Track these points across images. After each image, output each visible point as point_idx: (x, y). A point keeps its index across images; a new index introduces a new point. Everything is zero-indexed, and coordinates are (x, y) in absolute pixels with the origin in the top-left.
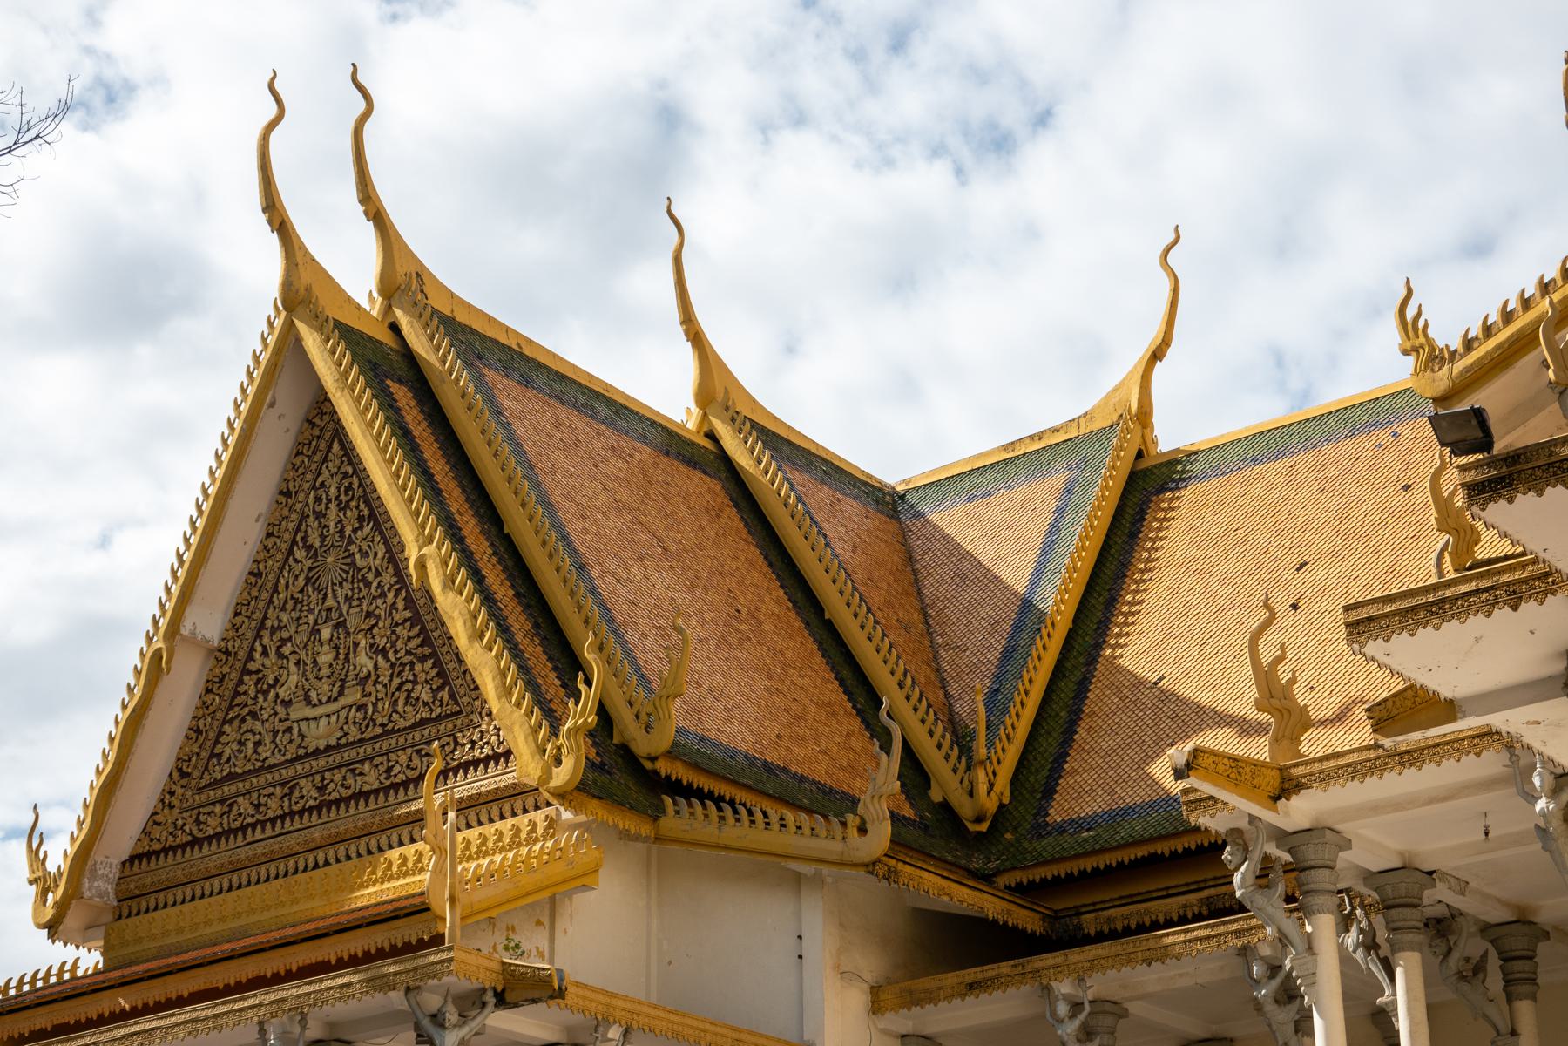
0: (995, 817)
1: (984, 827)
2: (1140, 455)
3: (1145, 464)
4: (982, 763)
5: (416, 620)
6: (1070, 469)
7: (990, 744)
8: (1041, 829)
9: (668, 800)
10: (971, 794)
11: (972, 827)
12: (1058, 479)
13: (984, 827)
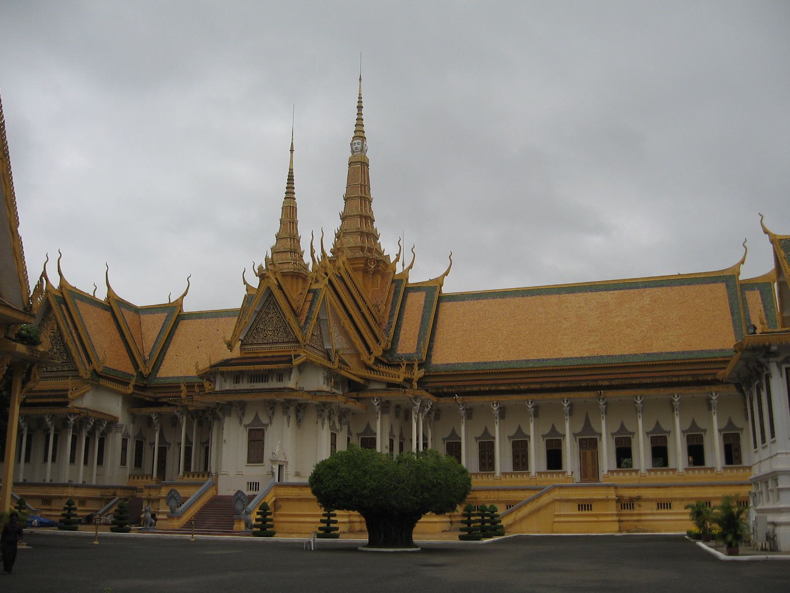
2: (180, 312)
3: (181, 313)
5: (64, 346)
8: (155, 378)
9: (101, 379)
12: (166, 314)
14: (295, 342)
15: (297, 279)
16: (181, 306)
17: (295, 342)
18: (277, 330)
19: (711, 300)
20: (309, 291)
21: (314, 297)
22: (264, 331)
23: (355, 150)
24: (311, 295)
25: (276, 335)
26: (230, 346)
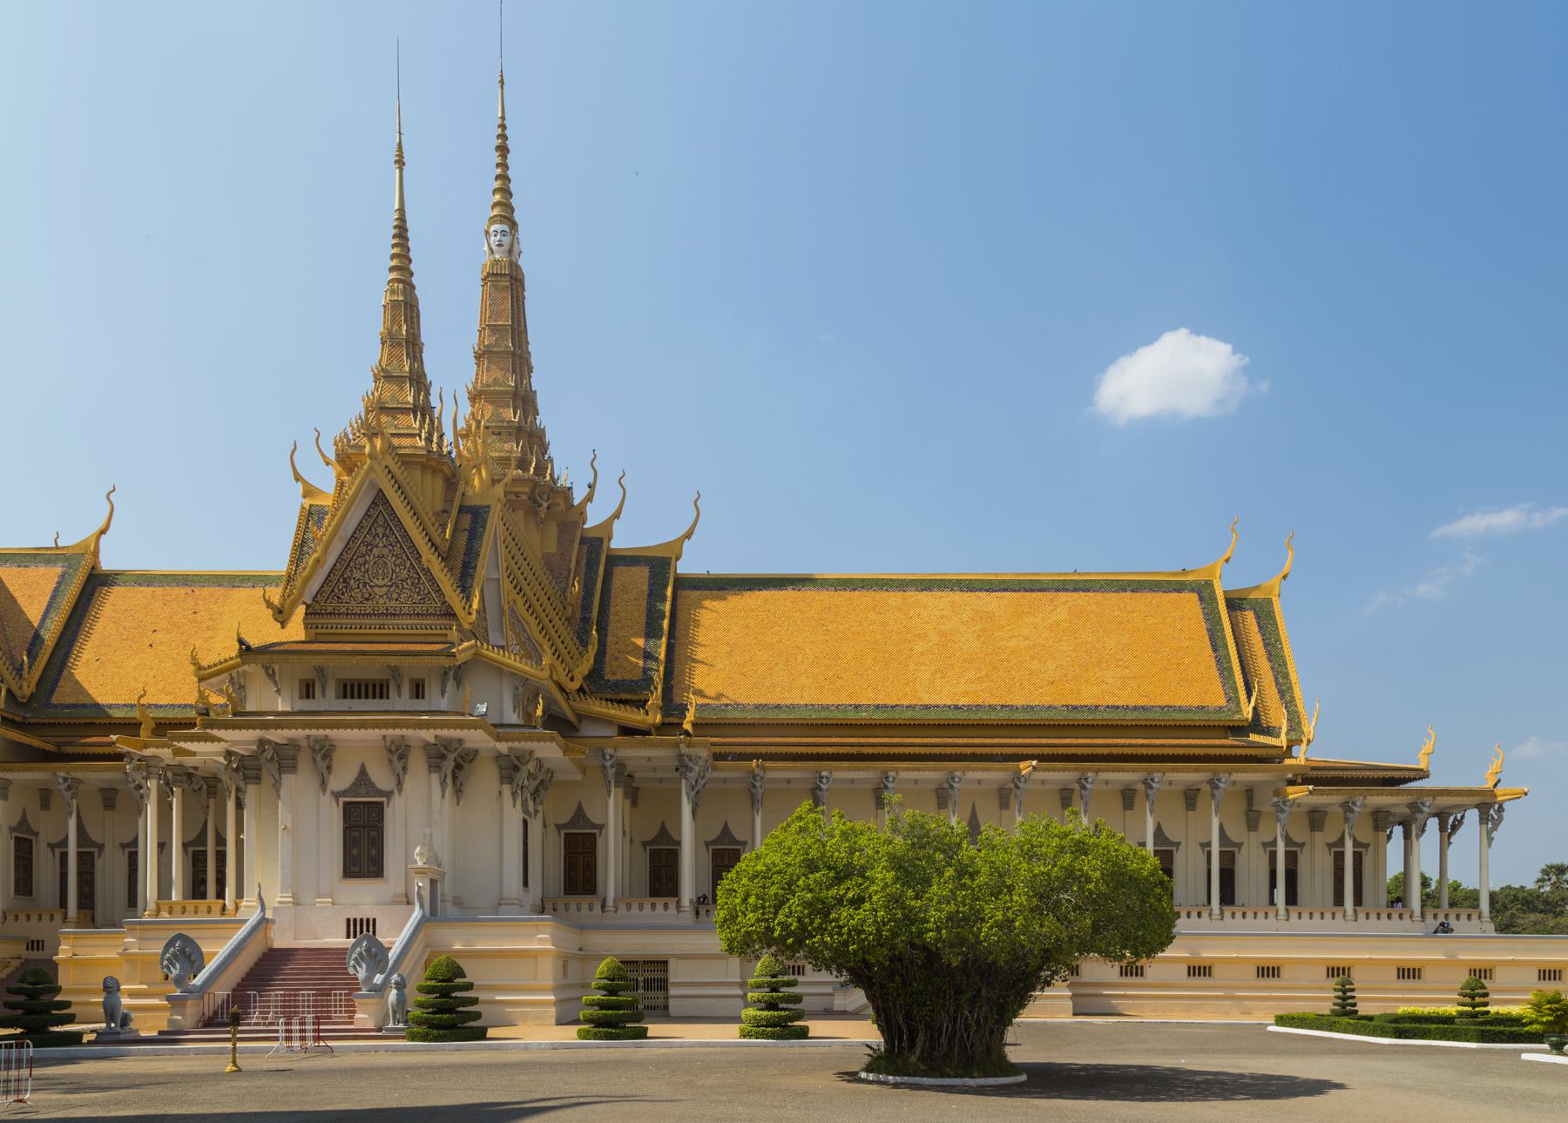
0: (30, 697)
1: (25, 700)
4: (26, 680)
6: (64, 567)
7: (29, 673)
10: (21, 688)
11: (21, 700)
12: (59, 570)
13: (25, 700)
14: (442, 615)
15: (433, 476)
16: (96, 553)
17: (442, 615)
18: (397, 586)
19: (1175, 621)
20: (462, 510)
21: (474, 522)
22: (364, 586)
23: (494, 248)
24: (467, 520)
25: (395, 596)
26: (281, 615)
